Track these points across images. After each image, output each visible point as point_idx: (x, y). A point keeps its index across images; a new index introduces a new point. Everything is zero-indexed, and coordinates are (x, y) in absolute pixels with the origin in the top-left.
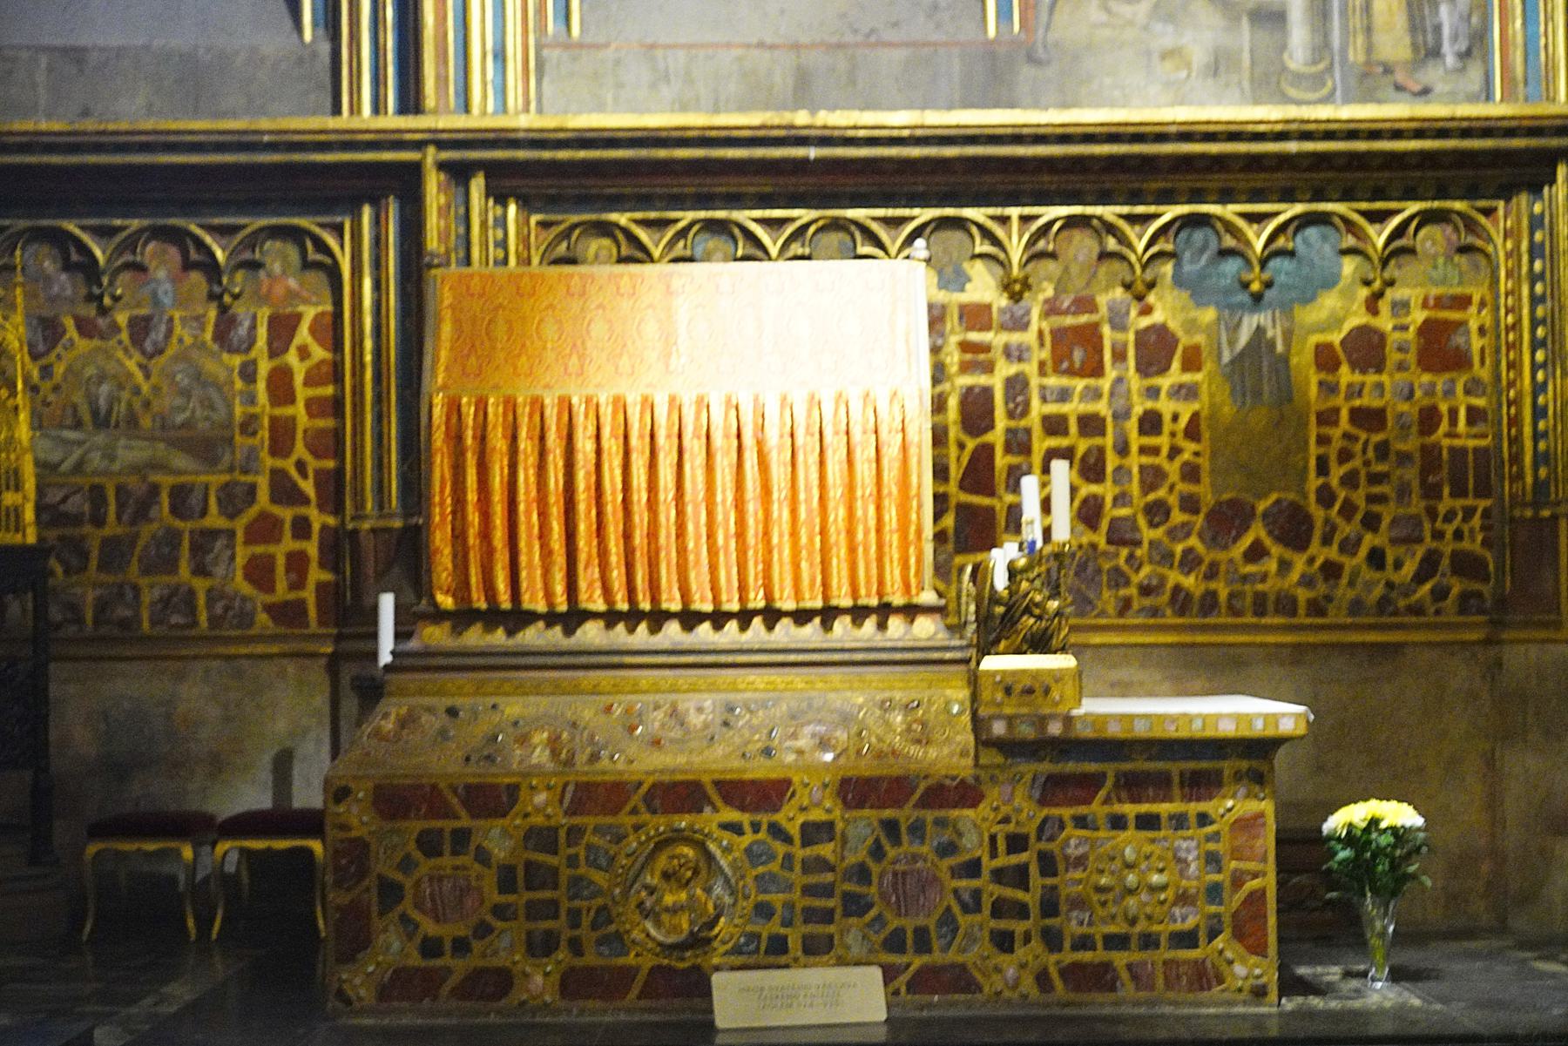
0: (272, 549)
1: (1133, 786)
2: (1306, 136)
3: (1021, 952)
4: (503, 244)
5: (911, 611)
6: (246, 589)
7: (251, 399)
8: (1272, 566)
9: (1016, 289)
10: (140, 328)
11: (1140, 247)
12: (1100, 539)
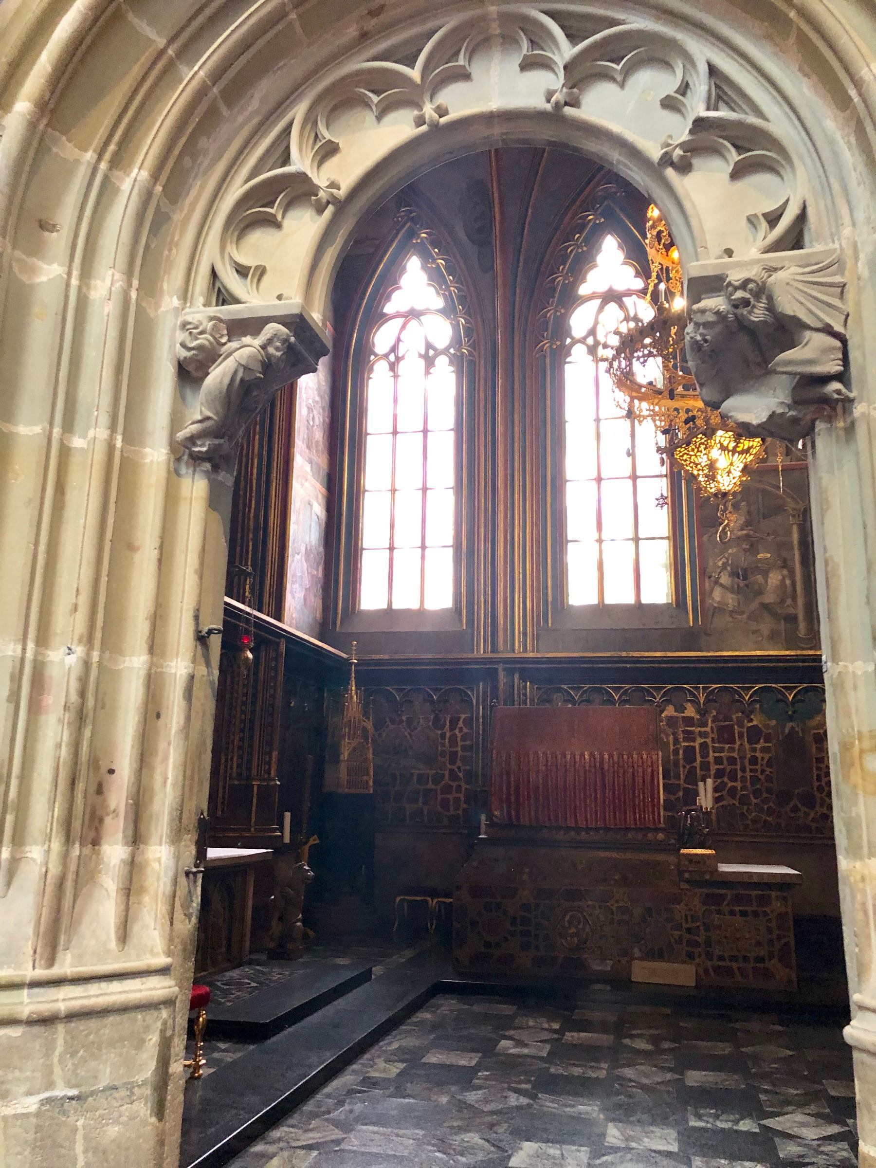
0: (448, 796)
1: (737, 899)
2: (803, 661)
3: (697, 960)
4: (525, 695)
5: (657, 830)
6: (439, 809)
7: (443, 745)
8: (802, 815)
9: (703, 712)
10: (409, 721)
11: (747, 698)
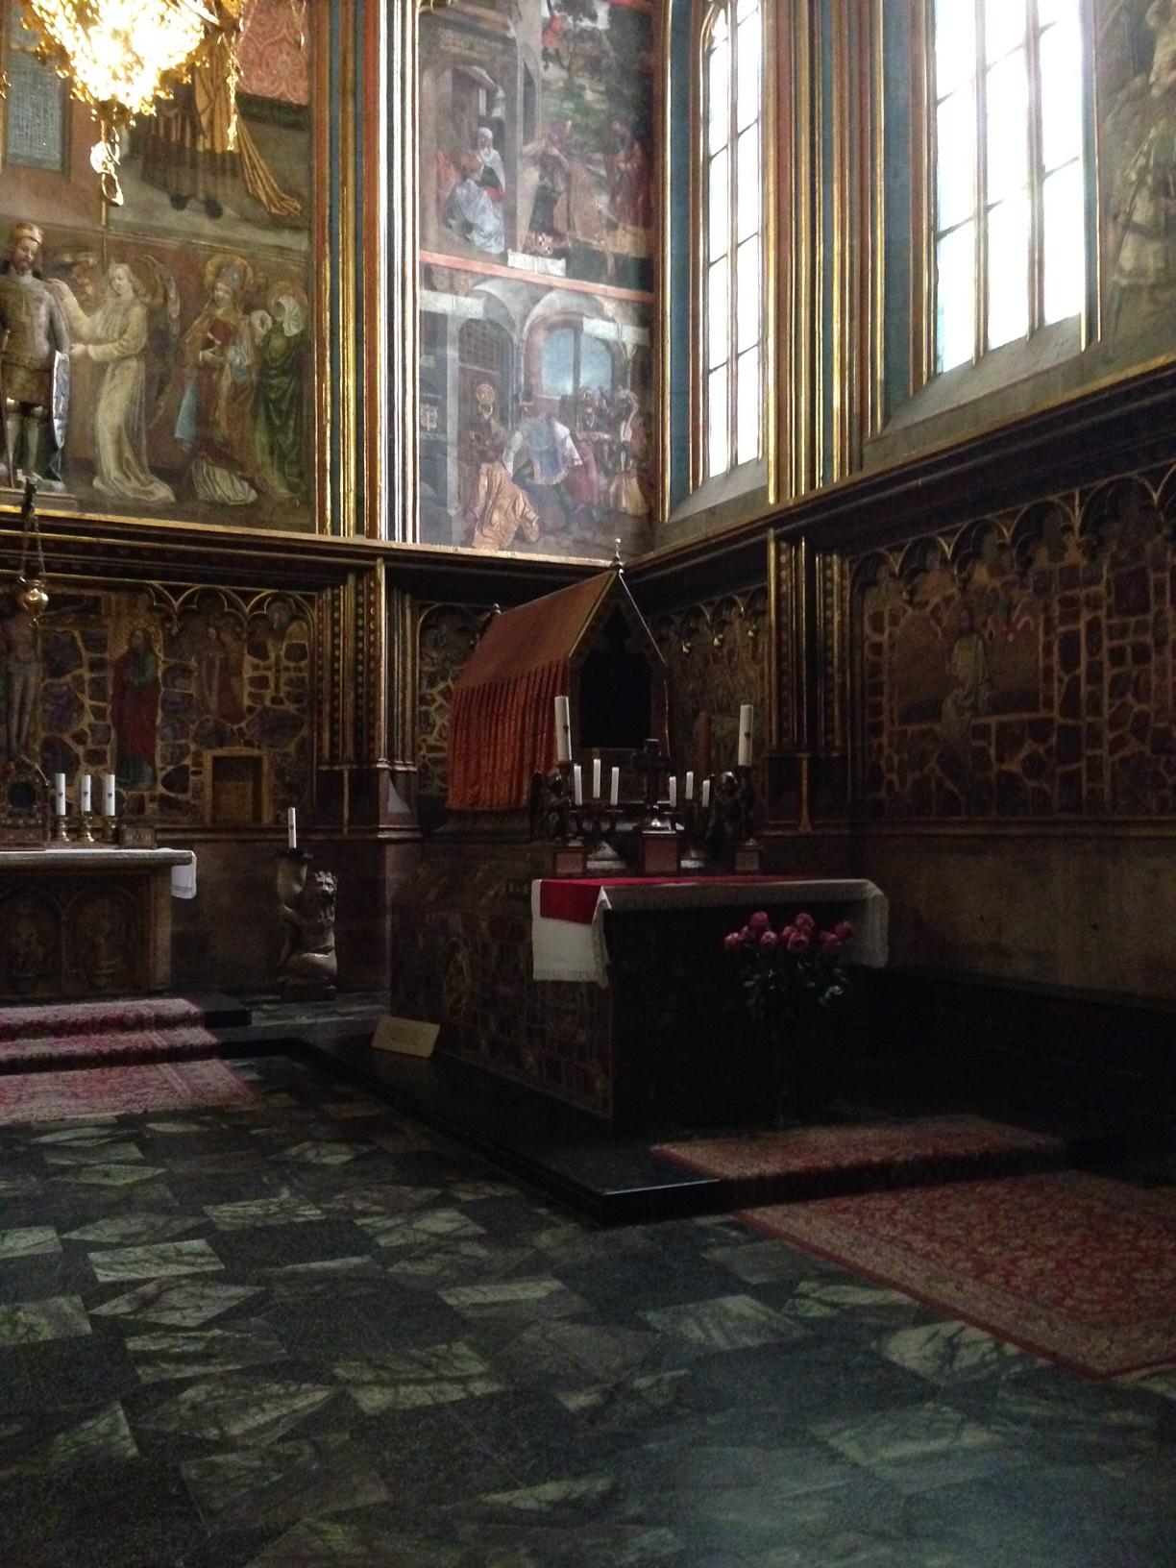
12: (1148, 751)
